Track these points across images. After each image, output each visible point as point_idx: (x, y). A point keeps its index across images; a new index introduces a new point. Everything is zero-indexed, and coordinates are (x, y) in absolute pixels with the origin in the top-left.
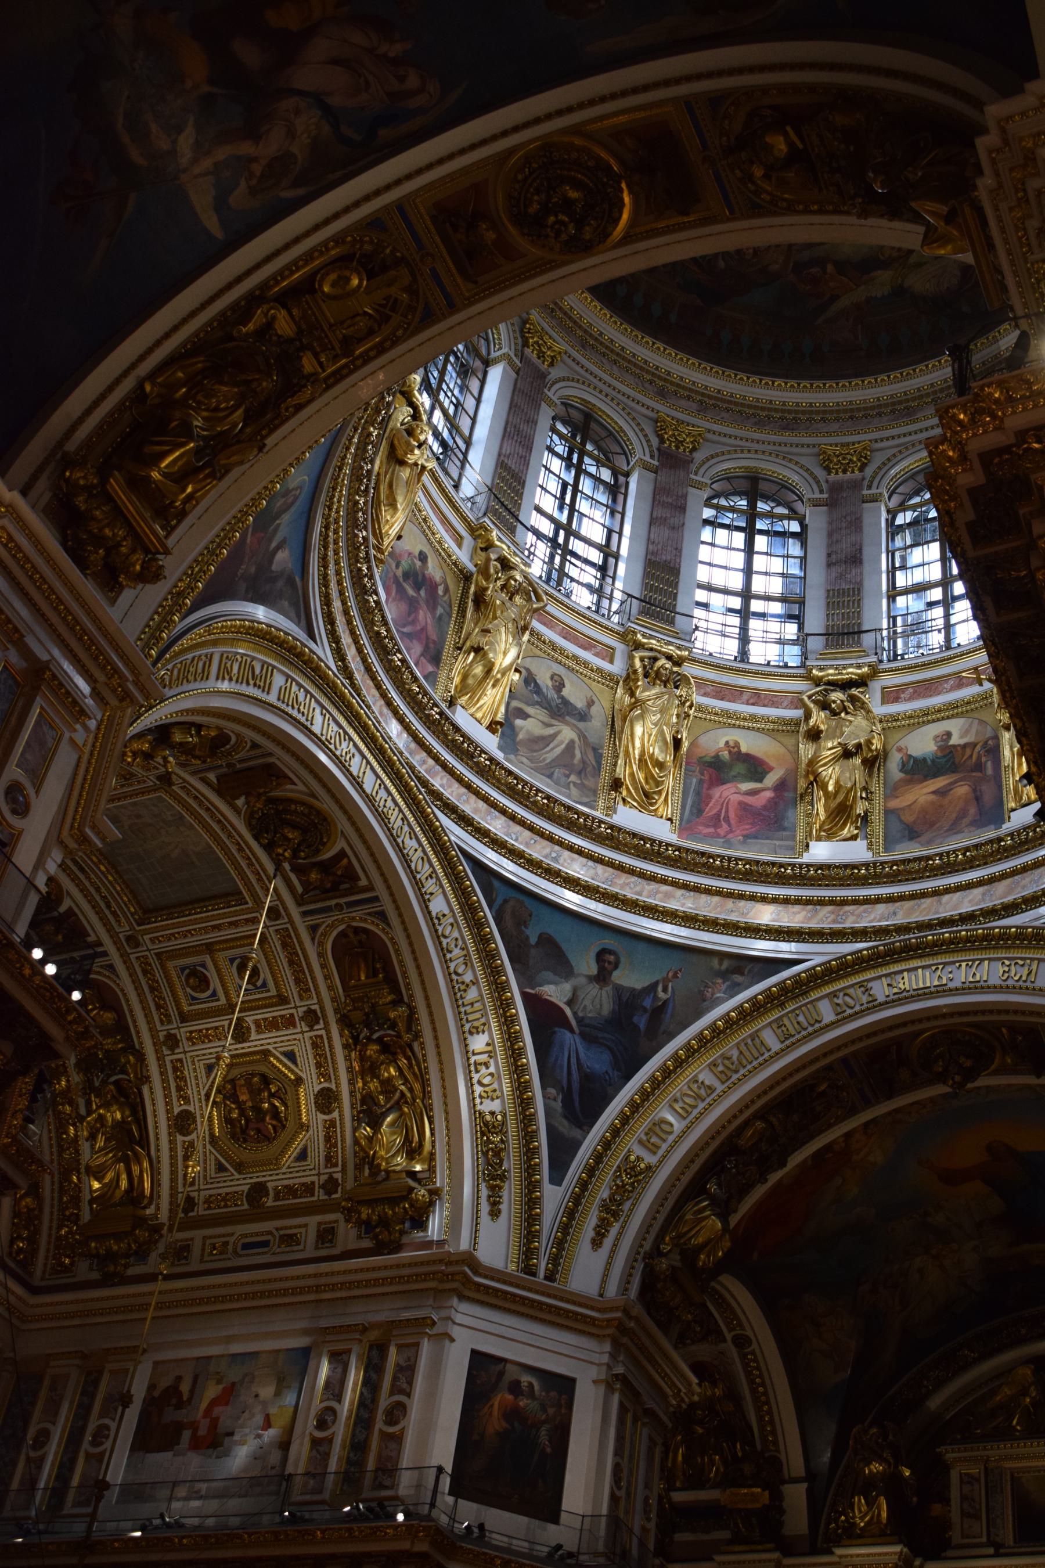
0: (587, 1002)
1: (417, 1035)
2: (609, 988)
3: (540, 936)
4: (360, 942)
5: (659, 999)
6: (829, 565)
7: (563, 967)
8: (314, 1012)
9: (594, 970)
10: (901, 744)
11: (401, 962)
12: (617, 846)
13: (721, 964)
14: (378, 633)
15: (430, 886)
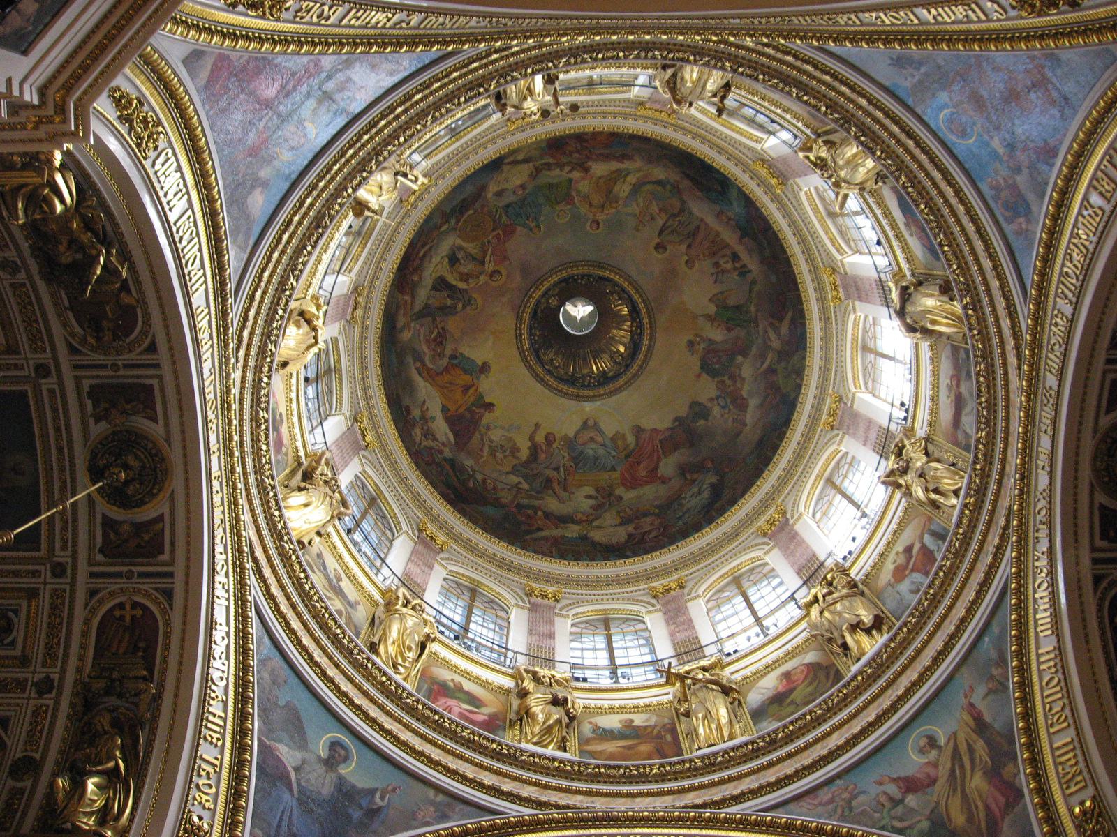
0: (312, 777)
1: (155, 718)
2: (334, 775)
3: (287, 705)
4: (133, 617)
5: (374, 803)
6: (530, 632)
7: (298, 734)
8: (52, 681)
9: (323, 753)
10: (593, 720)
11: (166, 648)
12: (369, 677)
13: (436, 796)
14: (261, 380)
15: (219, 591)
